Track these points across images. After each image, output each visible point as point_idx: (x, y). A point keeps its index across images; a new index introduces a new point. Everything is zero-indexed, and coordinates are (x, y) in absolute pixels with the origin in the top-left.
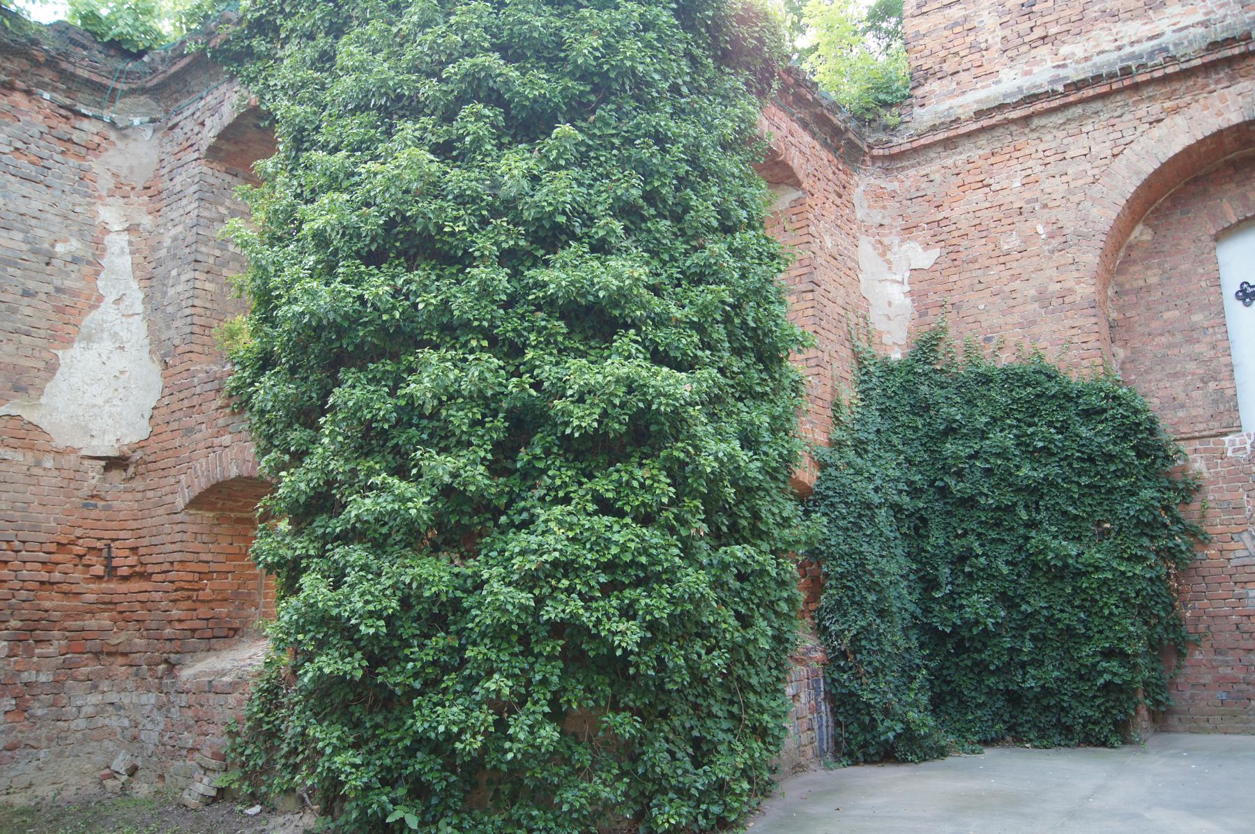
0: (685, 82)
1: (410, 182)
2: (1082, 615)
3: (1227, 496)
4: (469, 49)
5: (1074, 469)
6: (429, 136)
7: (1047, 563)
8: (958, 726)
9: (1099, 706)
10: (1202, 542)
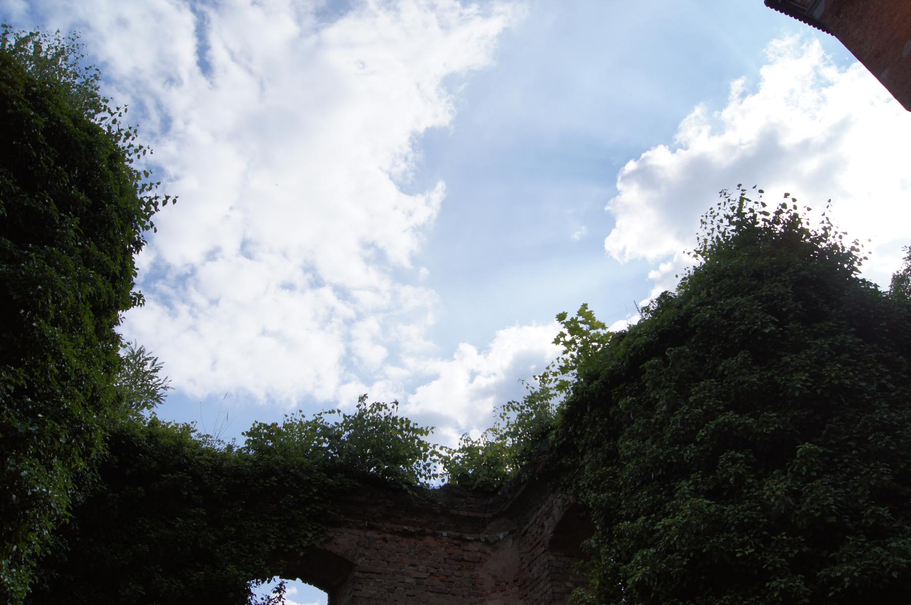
0: (888, 381)
1: (698, 525)
4: (710, 415)
6: (701, 487)
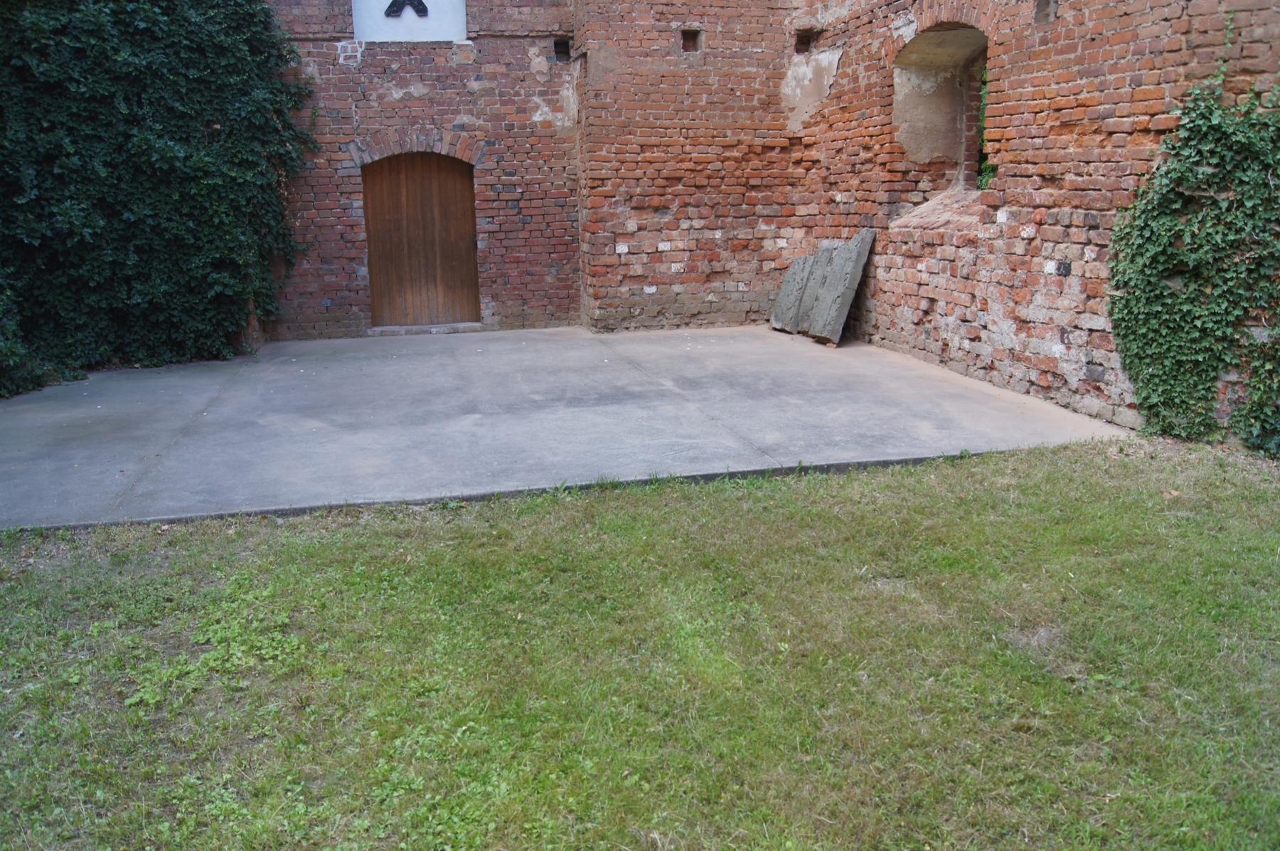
2: (191, 224)
3: (338, 105)
5: (181, 59)
7: (151, 165)
8: (55, 351)
9: (210, 320)
10: (310, 151)
